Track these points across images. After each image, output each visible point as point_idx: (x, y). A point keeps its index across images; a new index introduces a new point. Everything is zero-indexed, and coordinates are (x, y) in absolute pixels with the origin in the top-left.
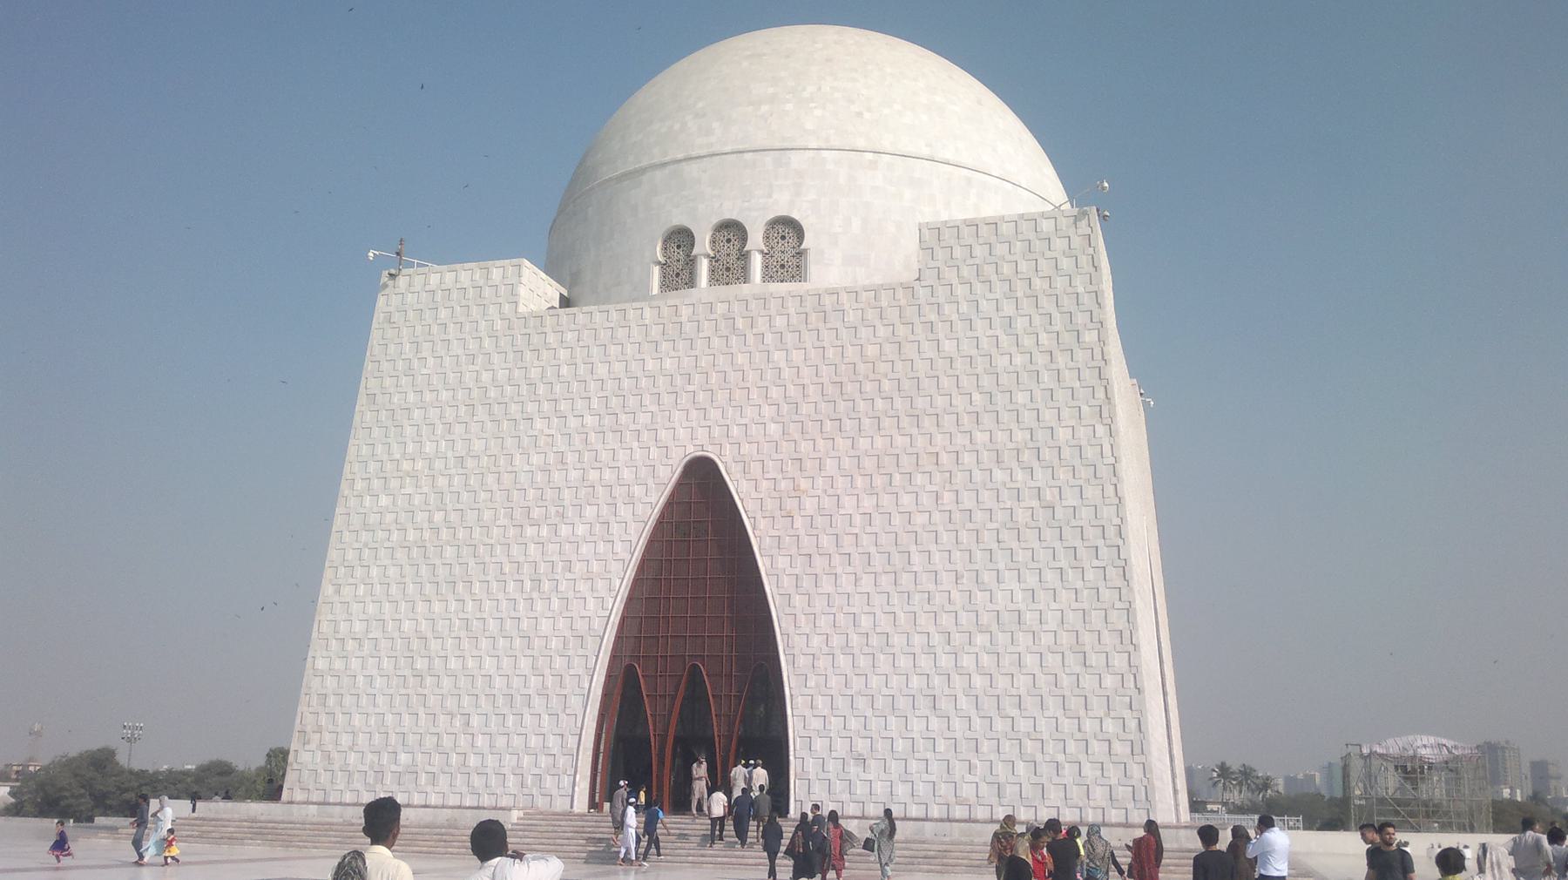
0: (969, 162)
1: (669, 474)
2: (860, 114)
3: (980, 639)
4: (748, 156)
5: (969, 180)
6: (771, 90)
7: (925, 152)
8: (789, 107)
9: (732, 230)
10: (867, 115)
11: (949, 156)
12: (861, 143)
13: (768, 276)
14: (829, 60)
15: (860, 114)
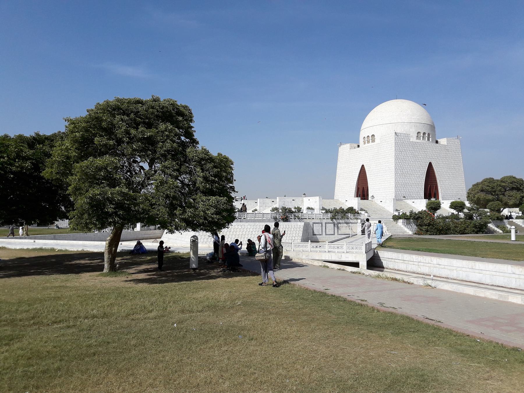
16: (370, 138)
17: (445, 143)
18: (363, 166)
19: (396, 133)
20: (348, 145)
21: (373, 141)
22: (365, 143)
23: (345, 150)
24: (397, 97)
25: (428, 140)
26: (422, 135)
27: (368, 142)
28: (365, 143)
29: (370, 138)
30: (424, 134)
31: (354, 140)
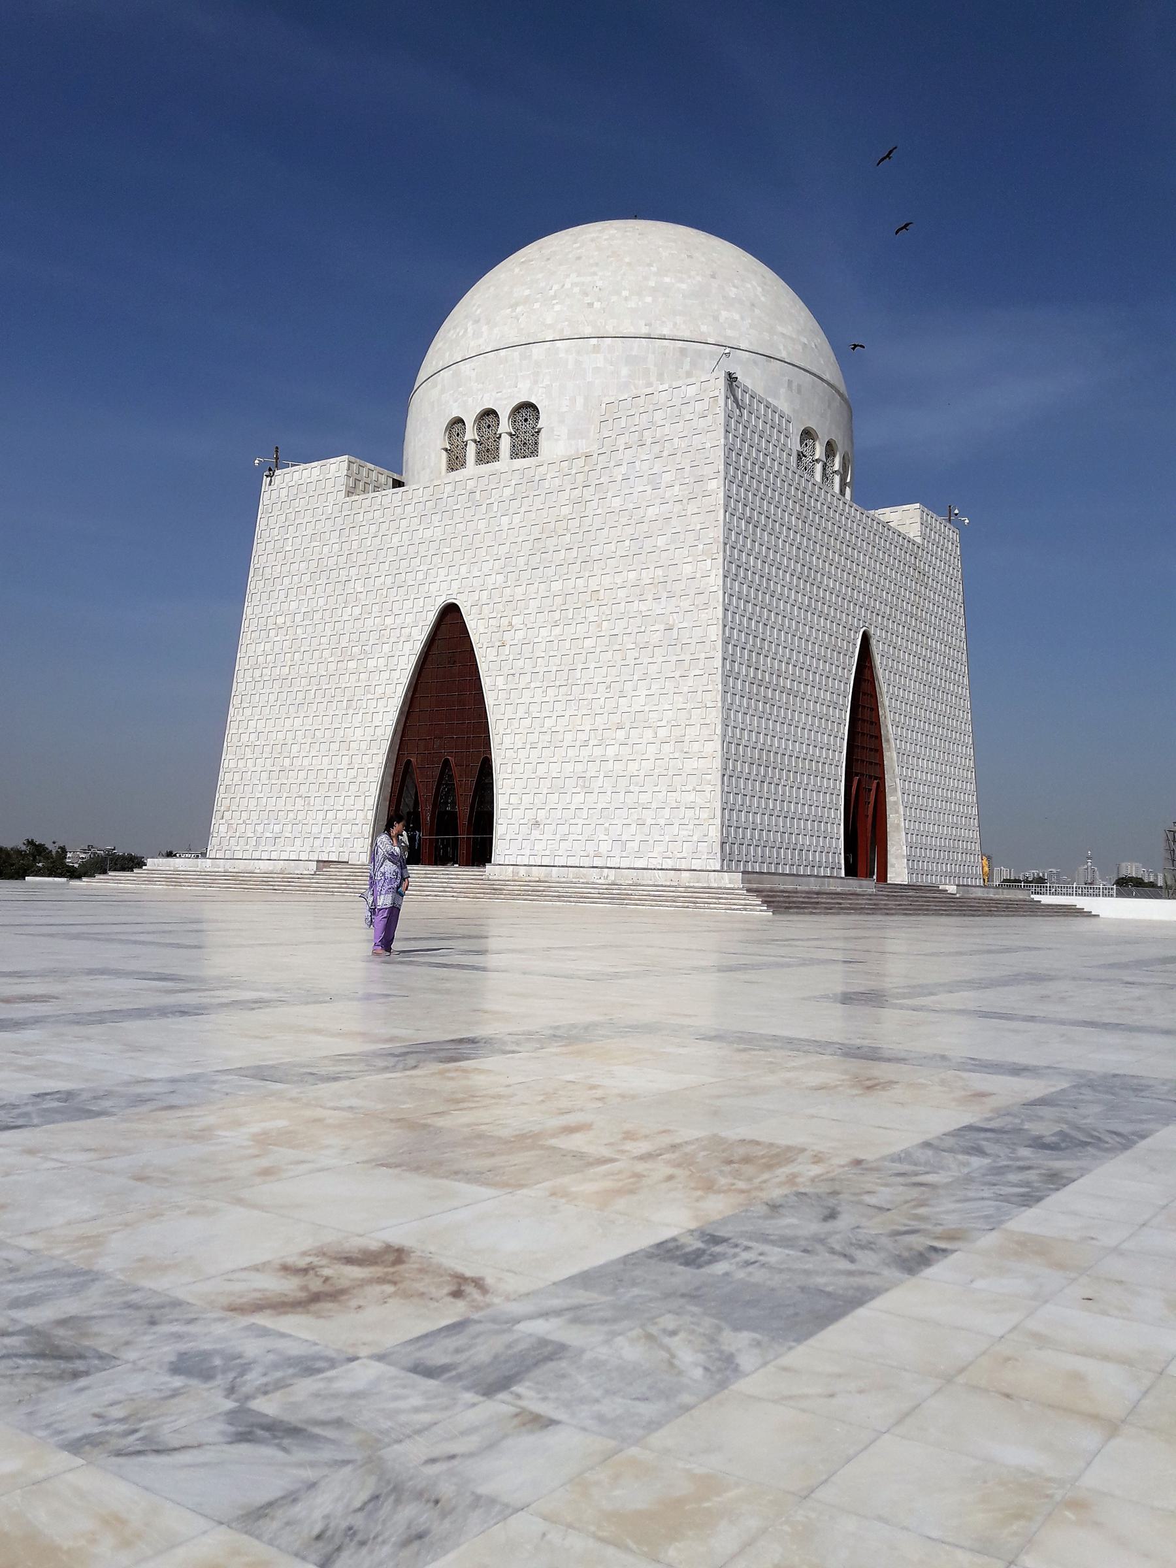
0: (687, 335)
1: (431, 617)
2: (591, 305)
3: (621, 734)
4: (503, 352)
5: (683, 351)
6: (527, 292)
7: (644, 331)
8: (537, 306)
9: (490, 413)
10: (597, 305)
11: (666, 331)
12: (588, 331)
13: (514, 455)
14: (579, 258)
15: (591, 305)
16: (505, 426)
17: (914, 531)
18: (450, 615)
19: (731, 378)
20: (337, 466)
21: (526, 446)
22: (455, 461)
23: (304, 504)
24: (636, 217)
25: (842, 492)
26: (819, 452)
27: (488, 454)
28: (455, 461)
29: (505, 426)
30: (830, 449)
31: (380, 447)
